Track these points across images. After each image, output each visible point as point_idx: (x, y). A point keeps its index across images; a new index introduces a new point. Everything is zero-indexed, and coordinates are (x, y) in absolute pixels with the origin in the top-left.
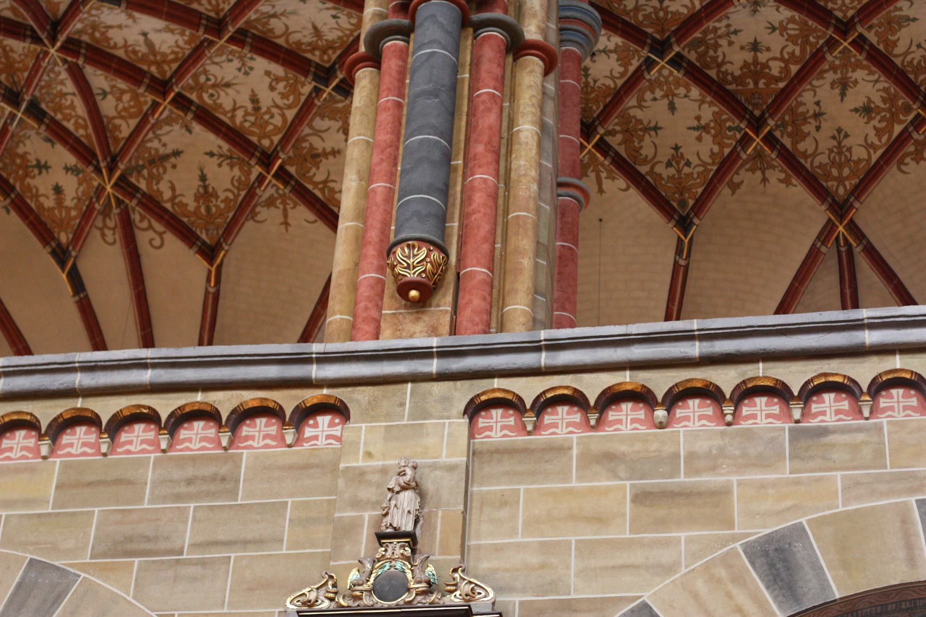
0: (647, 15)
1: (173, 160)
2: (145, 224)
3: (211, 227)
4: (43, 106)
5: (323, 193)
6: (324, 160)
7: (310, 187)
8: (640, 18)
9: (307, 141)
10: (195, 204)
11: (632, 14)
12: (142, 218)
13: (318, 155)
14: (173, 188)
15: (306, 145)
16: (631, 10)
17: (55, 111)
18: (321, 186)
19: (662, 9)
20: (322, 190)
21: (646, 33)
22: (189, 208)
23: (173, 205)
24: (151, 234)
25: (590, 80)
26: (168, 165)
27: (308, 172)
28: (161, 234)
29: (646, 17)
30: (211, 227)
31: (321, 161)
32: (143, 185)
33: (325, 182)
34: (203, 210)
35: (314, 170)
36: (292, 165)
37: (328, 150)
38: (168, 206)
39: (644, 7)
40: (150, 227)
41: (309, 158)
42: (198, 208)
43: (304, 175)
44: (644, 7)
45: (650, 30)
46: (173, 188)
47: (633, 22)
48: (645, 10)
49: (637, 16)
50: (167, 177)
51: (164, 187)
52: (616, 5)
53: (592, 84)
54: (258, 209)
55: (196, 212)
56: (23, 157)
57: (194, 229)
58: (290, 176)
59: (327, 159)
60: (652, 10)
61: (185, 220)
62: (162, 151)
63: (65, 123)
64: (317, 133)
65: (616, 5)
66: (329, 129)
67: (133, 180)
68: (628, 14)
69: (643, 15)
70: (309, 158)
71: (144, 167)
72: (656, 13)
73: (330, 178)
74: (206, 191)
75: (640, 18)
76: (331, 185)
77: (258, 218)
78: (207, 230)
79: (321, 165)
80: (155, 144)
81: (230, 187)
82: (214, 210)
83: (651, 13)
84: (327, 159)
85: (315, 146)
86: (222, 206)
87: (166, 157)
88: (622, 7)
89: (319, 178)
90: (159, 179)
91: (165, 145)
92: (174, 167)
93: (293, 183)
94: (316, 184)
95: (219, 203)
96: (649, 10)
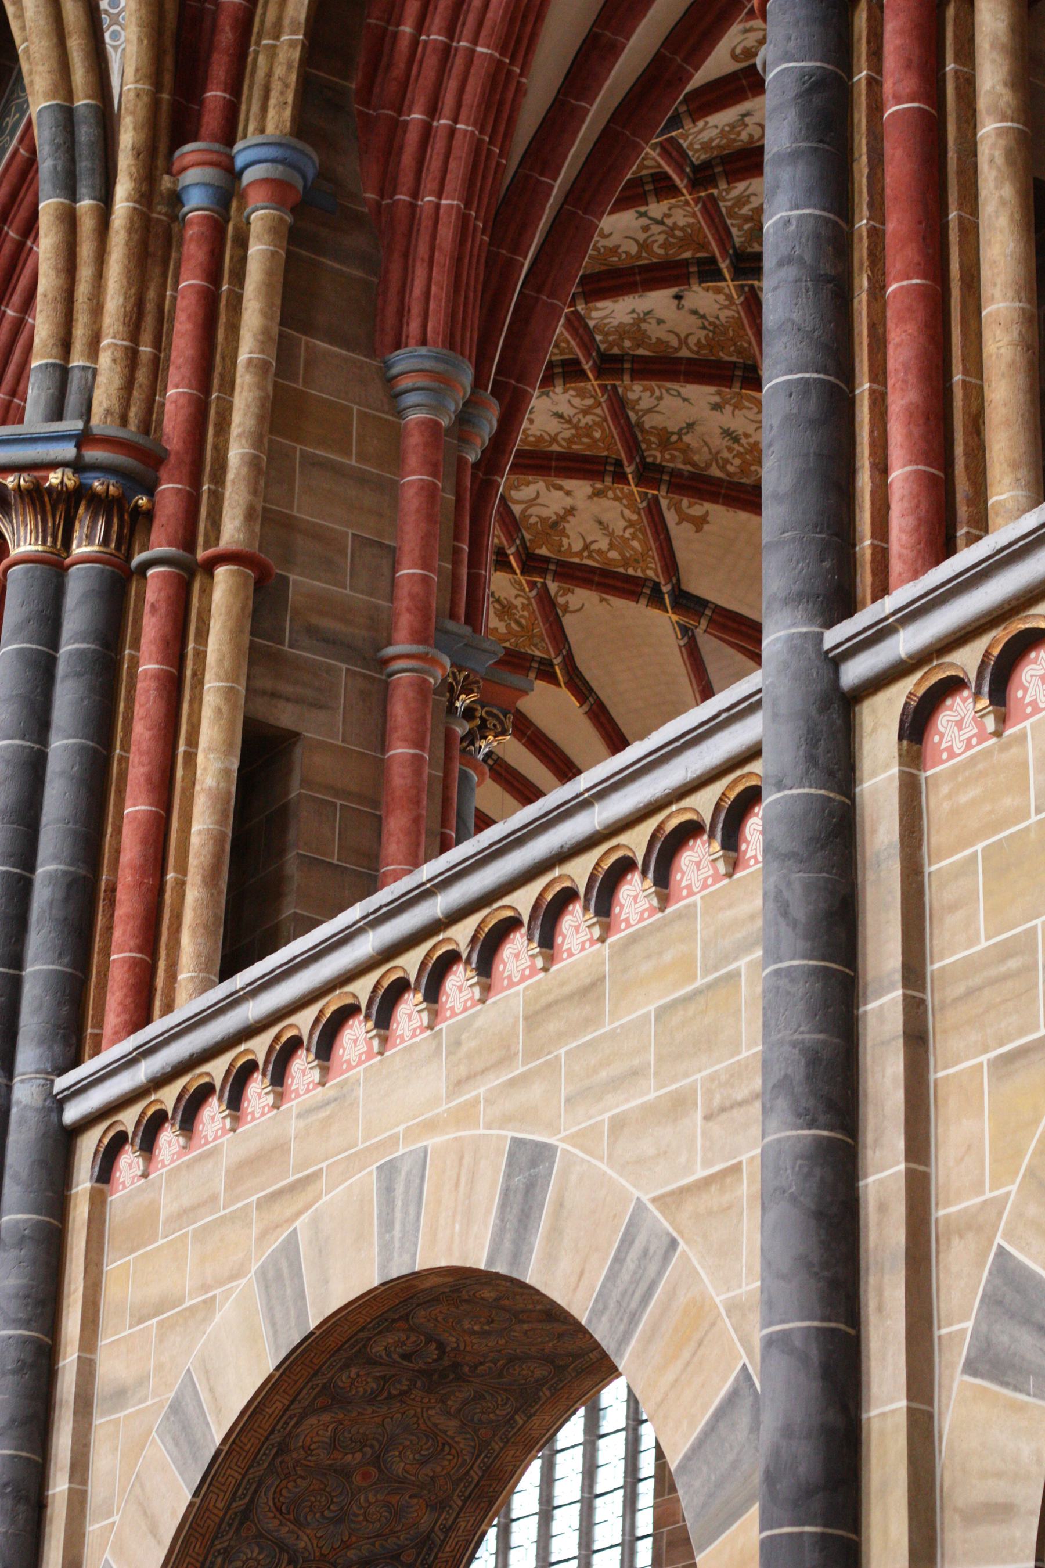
0: (664, 243)
3: (536, 640)
5: (594, 560)
6: (567, 525)
7: (576, 560)
8: (662, 252)
9: (531, 516)
10: (503, 624)
11: (644, 254)
13: (555, 525)
15: (533, 520)
16: (639, 252)
18: (585, 554)
19: (672, 229)
20: (590, 557)
21: (686, 260)
22: (500, 631)
25: (712, 319)
27: (561, 545)
29: (665, 245)
30: (536, 640)
31: (564, 527)
33: (586, 547)
34: (514, 625)
35: (565, 541)
36: (541, 548)
37: (562, 512)
39: (651, 239)
41: (549, 531)
42: (508, 626)
43: (560, 551)
44: (651, 239)
45: (687, 255)
47: (655, 260)
48: (656, 241)
49: (653, 251)
52: (616, 259)
53: (717, 322)
54: (561, 600)
55: (510, 632)
57: (522, 650)
58: (547, 560)
59: (568, 522)
60: (663, 237)
64: (532, 502)
65: (616, 259)
66: (538, 493)
68: (638, 256)
69: (660, 247)
70: (549, 531)
72: (673, 236)
73: (588, 541)
74: (503, 606)
75: (662, 252)
76: (594, 547)
77: (571, 607)
78: (535, 646)
79: (568, 531)
81: (517, 592)
82: (523, 621)
83: (666, 239)
84: (568, 522)
85: (544, 515)
86: (525, 613)
88: (624, 256)
89: (577, 546)
93: (552, 567)
94: (579, 554)
95: (521, 613)
96: (661, 239)
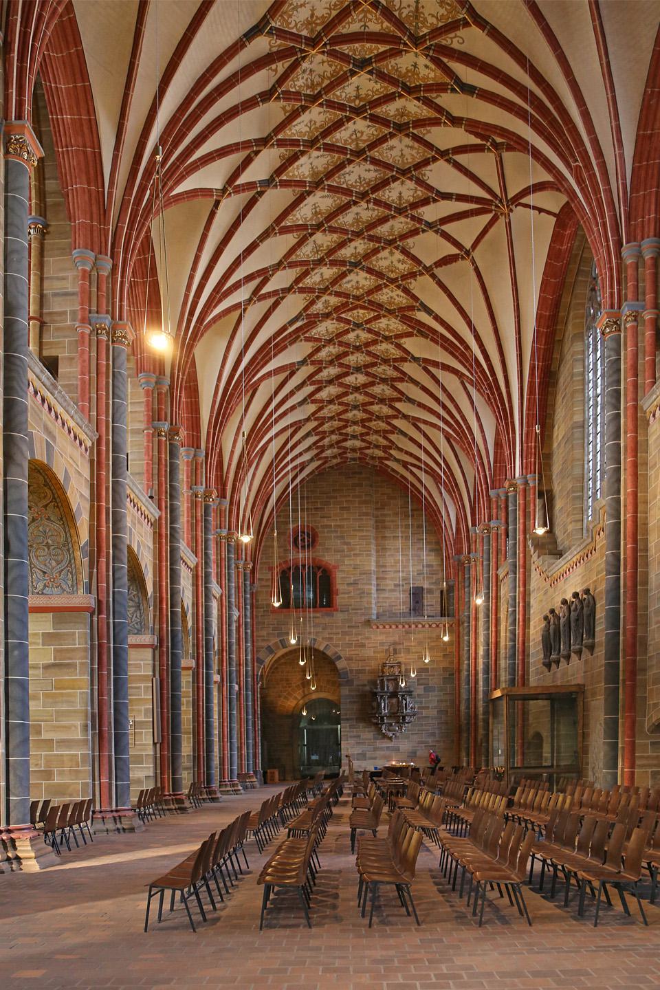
1: (420, 5)
2: (449, 41)
4: (367, 57)
12: (444, 39)
14: (433, 16)
17: (372, 53)
23: (440, 20)
24: (455, 40)
26: (421, 10)
28: (456, 36)
32: (426, 31)
38: (440, 24)
40: (451, 38)
42: (446, 9)
46: (433, 16)
50: (426, 15)
51: (431, 20)
56: (408, 71)
61: (450, 20)
62: (412, 9)
63: (380, 51)
67: (421, 34)
71: (417, 23)
80: (405, 12)
87: (417, 7)
90: (425, 19)
91: (409, 6)
92: (423, 7)
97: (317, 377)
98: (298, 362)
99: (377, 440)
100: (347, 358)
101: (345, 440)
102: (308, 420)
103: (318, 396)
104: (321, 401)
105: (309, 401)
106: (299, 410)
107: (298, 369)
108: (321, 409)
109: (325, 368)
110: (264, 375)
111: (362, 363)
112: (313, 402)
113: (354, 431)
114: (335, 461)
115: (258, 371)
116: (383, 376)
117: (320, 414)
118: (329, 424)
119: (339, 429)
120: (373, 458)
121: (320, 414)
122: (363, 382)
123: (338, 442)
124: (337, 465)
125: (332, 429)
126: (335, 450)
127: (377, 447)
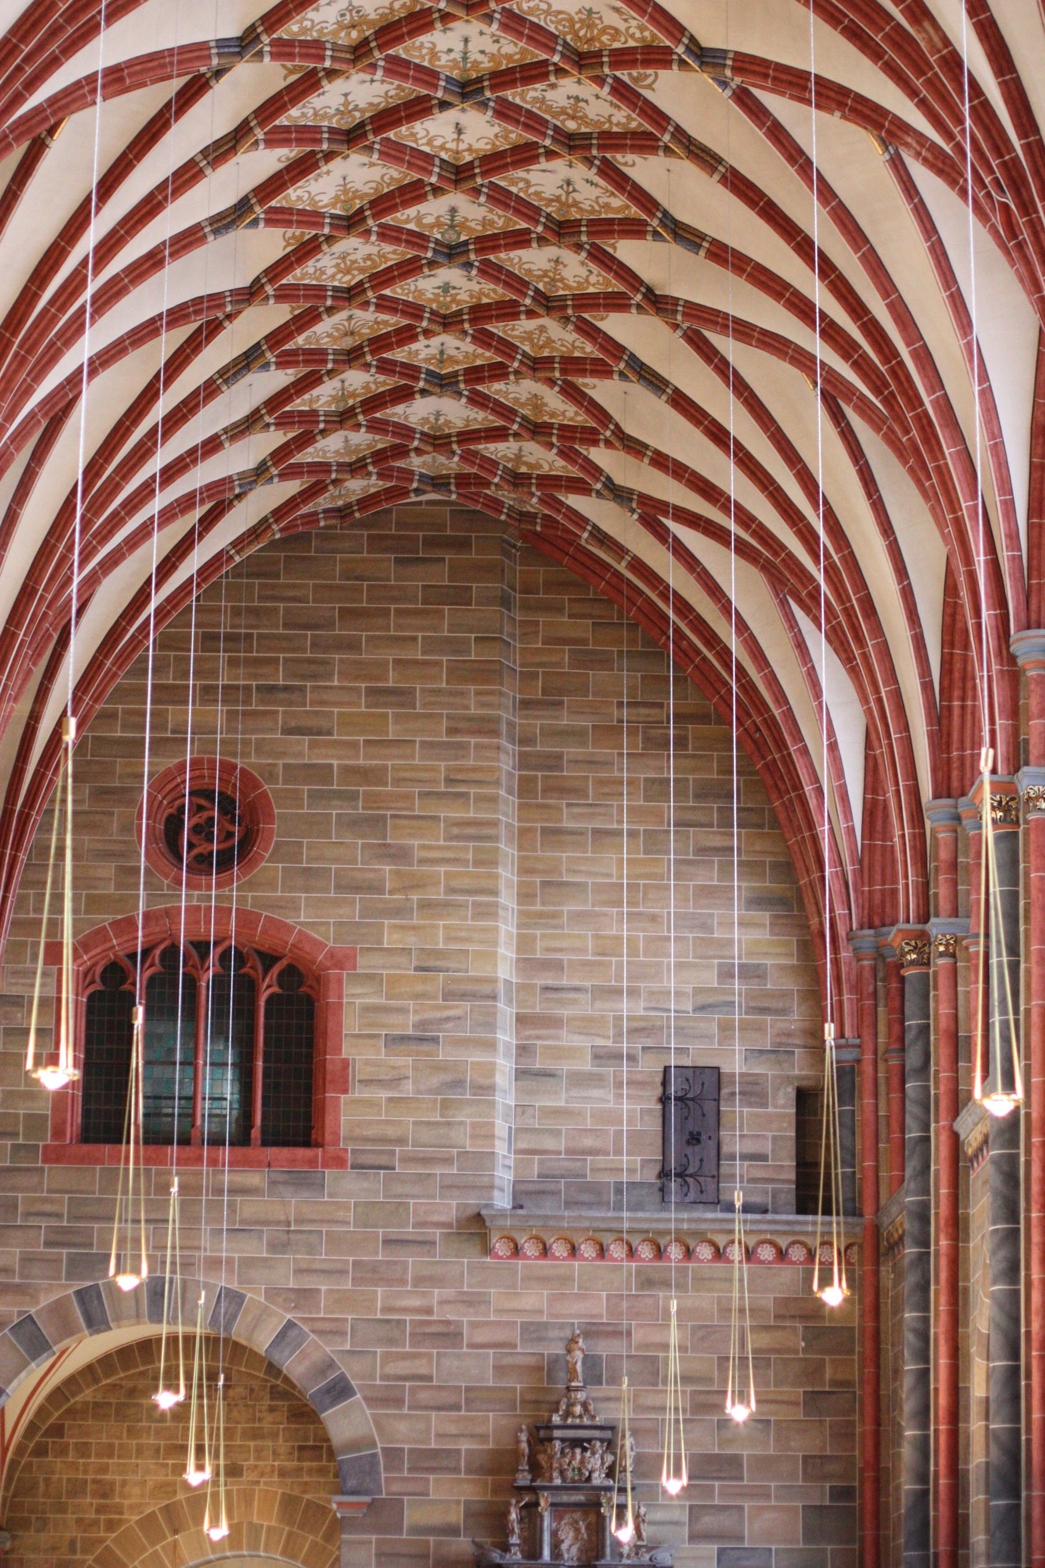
97: (294, 115)
98: (221, 43)
99: (536, 403)
100: (424, 39)
101: (402, 394)
102: (250, 294)
103: (296, 195)
104: (311, 217)
105: (260, 134)
106: (214, 247)
107: (219, 73)
108: (306, 250)
109: (332, 74)
110: (77, 85)
111: (487, 64)
112: (279, 218)
113: (442, 358)
114: (356, 487)
115: (54, 63)
116: (571, 125)
117: (304, 274)
118: (343, 315)
119: (380, 343)
120: (517, 480)
121: (304, 274)
122: (484, 147)
123: (374, 402)
124: (366, 502)
125: (348, 343)
126: (362, 439)
127: (538, 430)
